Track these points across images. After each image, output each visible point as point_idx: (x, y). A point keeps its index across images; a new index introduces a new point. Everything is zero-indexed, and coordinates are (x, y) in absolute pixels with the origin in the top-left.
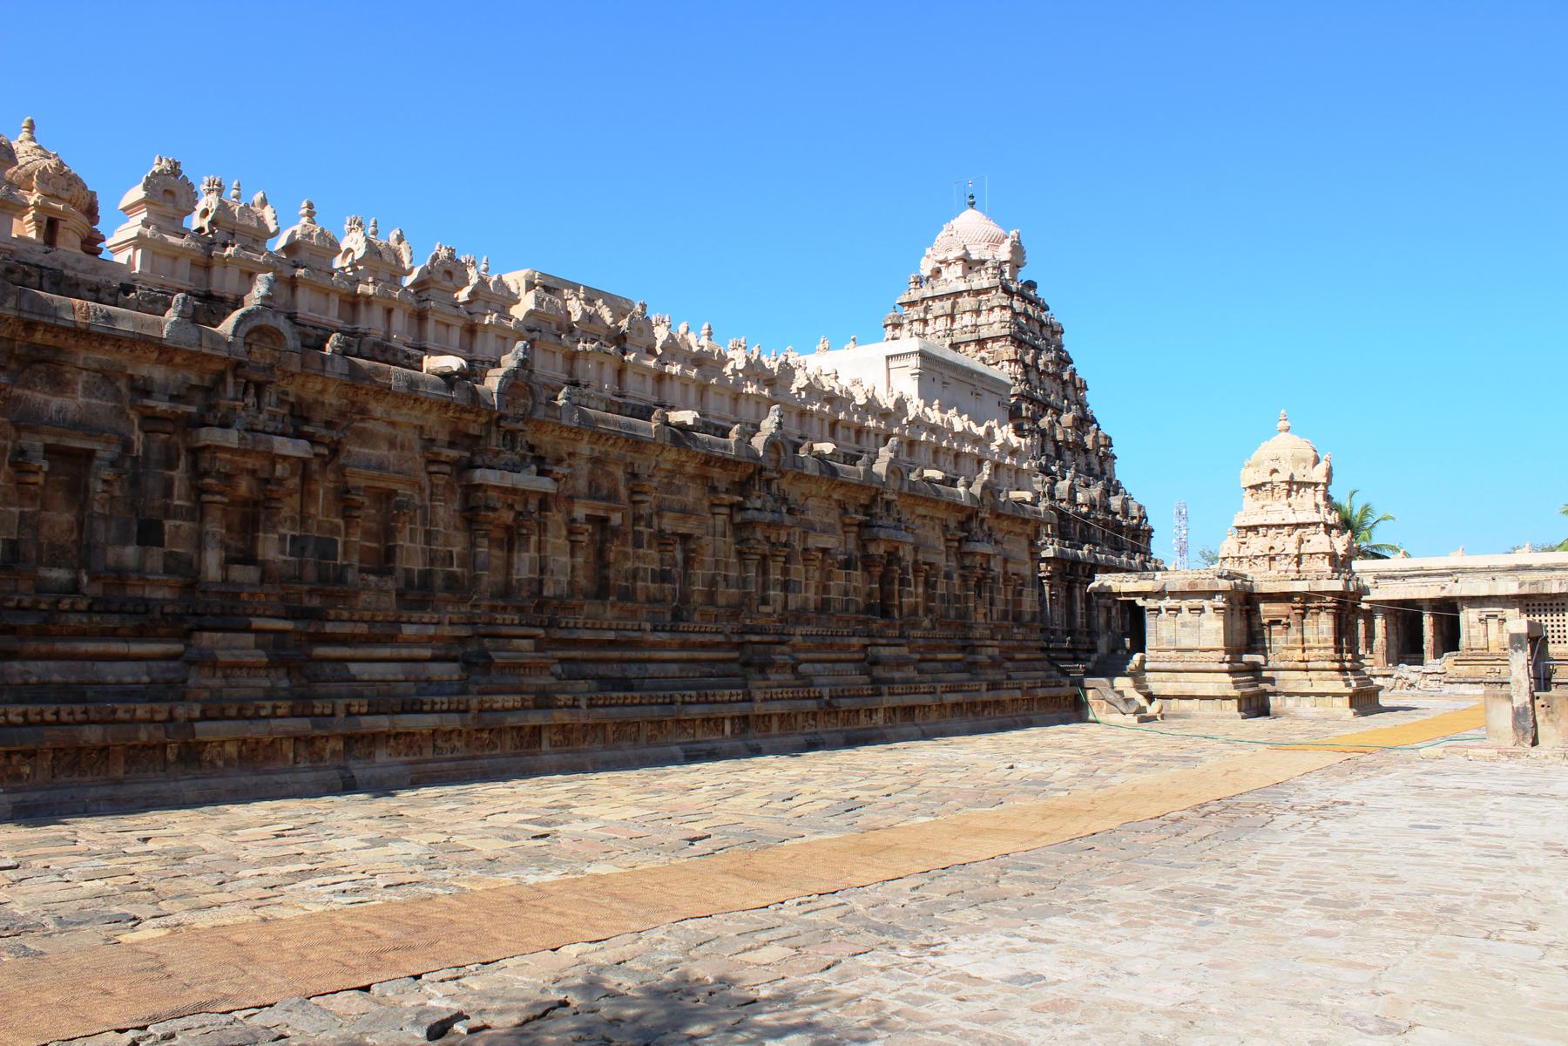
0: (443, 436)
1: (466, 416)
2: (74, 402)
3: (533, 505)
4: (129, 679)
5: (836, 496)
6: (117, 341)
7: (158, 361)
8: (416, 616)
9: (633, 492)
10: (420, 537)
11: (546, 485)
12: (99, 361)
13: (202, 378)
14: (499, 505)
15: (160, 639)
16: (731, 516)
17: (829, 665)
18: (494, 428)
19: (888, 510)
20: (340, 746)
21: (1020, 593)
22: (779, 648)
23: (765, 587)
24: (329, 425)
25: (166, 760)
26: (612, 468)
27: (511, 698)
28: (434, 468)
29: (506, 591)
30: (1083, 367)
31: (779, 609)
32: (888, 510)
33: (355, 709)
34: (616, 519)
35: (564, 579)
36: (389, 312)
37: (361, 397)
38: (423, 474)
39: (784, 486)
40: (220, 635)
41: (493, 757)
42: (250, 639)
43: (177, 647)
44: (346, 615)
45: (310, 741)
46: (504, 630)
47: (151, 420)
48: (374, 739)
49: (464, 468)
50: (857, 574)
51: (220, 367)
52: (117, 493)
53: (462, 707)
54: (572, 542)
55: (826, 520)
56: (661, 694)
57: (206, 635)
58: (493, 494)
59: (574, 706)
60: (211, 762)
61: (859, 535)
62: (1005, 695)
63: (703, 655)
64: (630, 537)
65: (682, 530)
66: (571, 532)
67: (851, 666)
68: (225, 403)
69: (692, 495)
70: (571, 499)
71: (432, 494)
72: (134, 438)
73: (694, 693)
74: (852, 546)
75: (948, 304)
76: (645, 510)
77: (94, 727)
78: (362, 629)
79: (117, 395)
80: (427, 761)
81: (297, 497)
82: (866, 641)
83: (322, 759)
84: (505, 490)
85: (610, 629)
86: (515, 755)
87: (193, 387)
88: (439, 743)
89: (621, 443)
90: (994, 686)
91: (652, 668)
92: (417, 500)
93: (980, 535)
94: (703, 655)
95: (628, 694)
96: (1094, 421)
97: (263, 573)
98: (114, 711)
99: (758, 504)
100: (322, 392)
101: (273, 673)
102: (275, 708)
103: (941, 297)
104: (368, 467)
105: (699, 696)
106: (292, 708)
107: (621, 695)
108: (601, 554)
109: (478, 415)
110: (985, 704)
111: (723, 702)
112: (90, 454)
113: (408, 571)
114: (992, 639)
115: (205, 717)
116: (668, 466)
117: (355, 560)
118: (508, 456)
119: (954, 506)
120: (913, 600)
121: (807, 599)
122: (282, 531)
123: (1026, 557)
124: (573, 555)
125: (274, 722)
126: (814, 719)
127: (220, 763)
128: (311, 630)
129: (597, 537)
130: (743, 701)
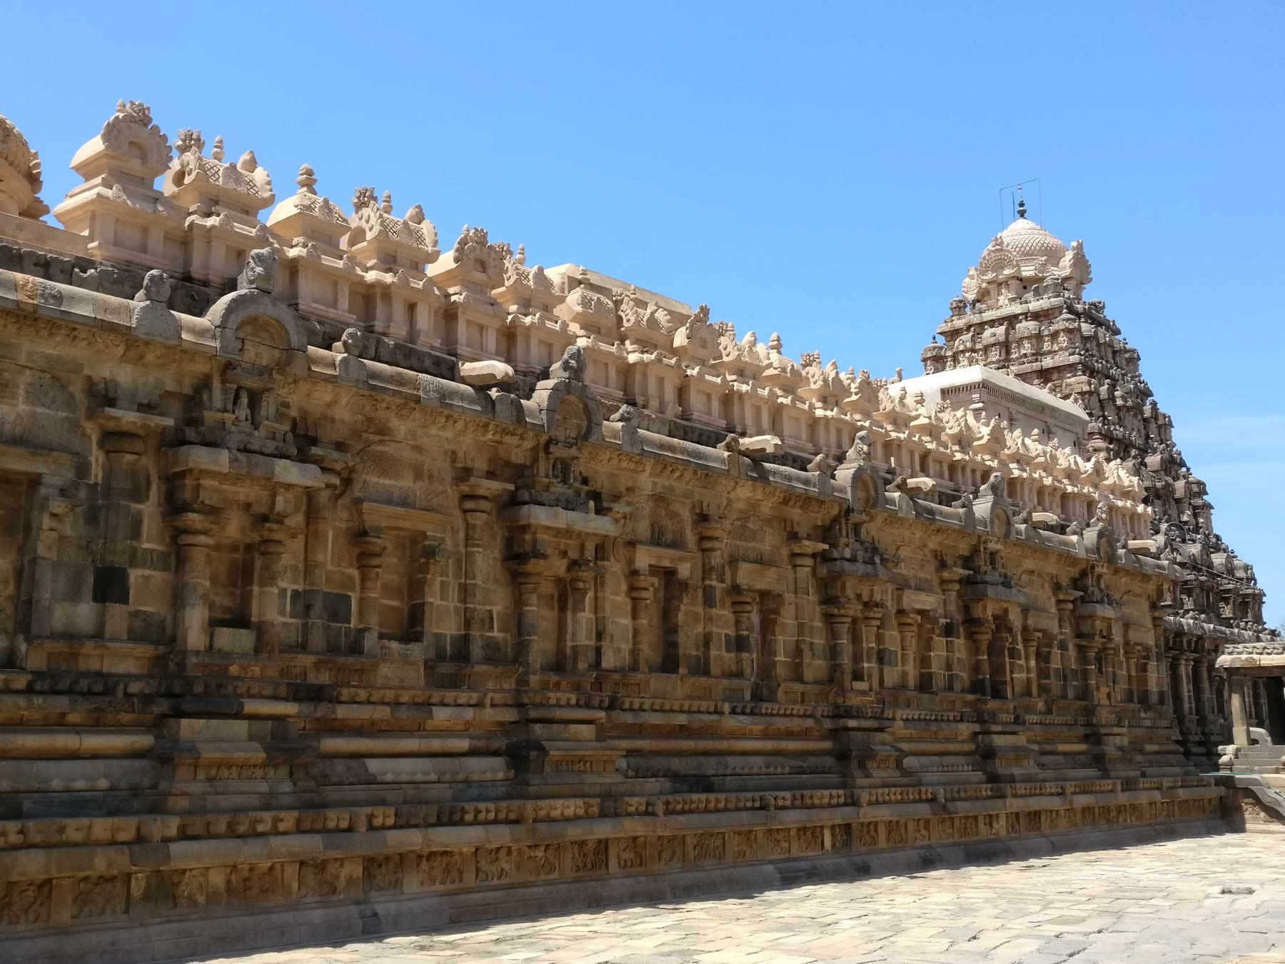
0: (481, 465)
1: (508, 439)
2: (13, 411)
3: (590, 553)
4: (80, 784)
5: (932, 546)
6: (68, 326)
7: (124, 359)
8: (450, 696)
9: (702, 539)
10: (454, 593)
11: (602, 526)
12: (46, 356)
13: (179, 383)
14: (549, 551)
15: (120, 728)
16: (814, 569)
17: (936, 759)
18: (542, 455)
19: (993, 563)
20: (358, 871)
21: (1144, 668)
22: (879, 736)
24: (340, 446)
25: (128, 897)
26: (677, 507)
27: (572, 802)
28: (469, 505)
29: (559, 664)
30: (1165, 400)
31: (876, 685)
32: (993, 563)
33: (378, 822)
34: (684, 570)
35: (626, 647)
36: (412, 308)
37: (381, 414)
38: (457, 513)
39: (873, 533)
40: (202, 722)
41: (551, 883)
42: (241, 727)
43: (145, 741)
44: (363, 694)
45: (321, 866)
46: (559, 714)
47: (113, 438)
48: (402, 861)
49: (512, 502)
50: (960, 642)
51: (202, 367)
52: (68, 532)
53: (512, 816)
54: (633, 599)
55: (921, 575)
56: (749, 795)
57: (184, 722)
59: (647, 813)
60: (190, 898)
61: (960, 595)
62: (1143, 798)
63: (792, 745)
64: (700, 592)
65: (760, 586)
66: (632, 588)
67: (961, 759)
68: (210, 416)
69: (769, 542)
70: (631, 544)
71: (467, 538)
72: (93, 459)
73: (788, 795)
74: (952, 608)
75: (1001, 330)
76: (717, 559)
77: (33, 852)
78: (383, 713)
79: (70, 403)
80: (468, 891)
81: (301, 537)
82: (977, 728)
83: (334, 890)
84: (557, 532)
85: (682, 711)
86: (577, 880)
87: (170, 394)
88: (483, 864)
89: (688, 474)
90: (1128, 785)
91: (733, 761)
92: (449, 544)
93: (1098, 595)
94: (792, 745)
95: (712, 796)
96: (1182, 464)
97: (260, 638)
98: (62, 830)
99: (847, 553)
101: (271, 772)
102: (276, 821)
103: (992, 323)
104: (389, 502)
105: (794, 798)
106: (299, 821)
107: (703, 796)
108: (667, 615)
109: (522, 438)
110: (1120, 810)
111: (822, 807)
112: (34, 481)
114: (1119, 725)
115: (184, 836)
116: (741, 505)
117: (373, 620)
118: (559, 489)
119: (1067, 558)
120: (1024, 676)
121: (904, 675)
122: (283, 584)
123: (1148, 622)
124: (635, 615)
125: (275, 841)
126: (927, 828)
127: (201, 899)
128: (319, 714)
129: (661, 594)
130: (845, 804)
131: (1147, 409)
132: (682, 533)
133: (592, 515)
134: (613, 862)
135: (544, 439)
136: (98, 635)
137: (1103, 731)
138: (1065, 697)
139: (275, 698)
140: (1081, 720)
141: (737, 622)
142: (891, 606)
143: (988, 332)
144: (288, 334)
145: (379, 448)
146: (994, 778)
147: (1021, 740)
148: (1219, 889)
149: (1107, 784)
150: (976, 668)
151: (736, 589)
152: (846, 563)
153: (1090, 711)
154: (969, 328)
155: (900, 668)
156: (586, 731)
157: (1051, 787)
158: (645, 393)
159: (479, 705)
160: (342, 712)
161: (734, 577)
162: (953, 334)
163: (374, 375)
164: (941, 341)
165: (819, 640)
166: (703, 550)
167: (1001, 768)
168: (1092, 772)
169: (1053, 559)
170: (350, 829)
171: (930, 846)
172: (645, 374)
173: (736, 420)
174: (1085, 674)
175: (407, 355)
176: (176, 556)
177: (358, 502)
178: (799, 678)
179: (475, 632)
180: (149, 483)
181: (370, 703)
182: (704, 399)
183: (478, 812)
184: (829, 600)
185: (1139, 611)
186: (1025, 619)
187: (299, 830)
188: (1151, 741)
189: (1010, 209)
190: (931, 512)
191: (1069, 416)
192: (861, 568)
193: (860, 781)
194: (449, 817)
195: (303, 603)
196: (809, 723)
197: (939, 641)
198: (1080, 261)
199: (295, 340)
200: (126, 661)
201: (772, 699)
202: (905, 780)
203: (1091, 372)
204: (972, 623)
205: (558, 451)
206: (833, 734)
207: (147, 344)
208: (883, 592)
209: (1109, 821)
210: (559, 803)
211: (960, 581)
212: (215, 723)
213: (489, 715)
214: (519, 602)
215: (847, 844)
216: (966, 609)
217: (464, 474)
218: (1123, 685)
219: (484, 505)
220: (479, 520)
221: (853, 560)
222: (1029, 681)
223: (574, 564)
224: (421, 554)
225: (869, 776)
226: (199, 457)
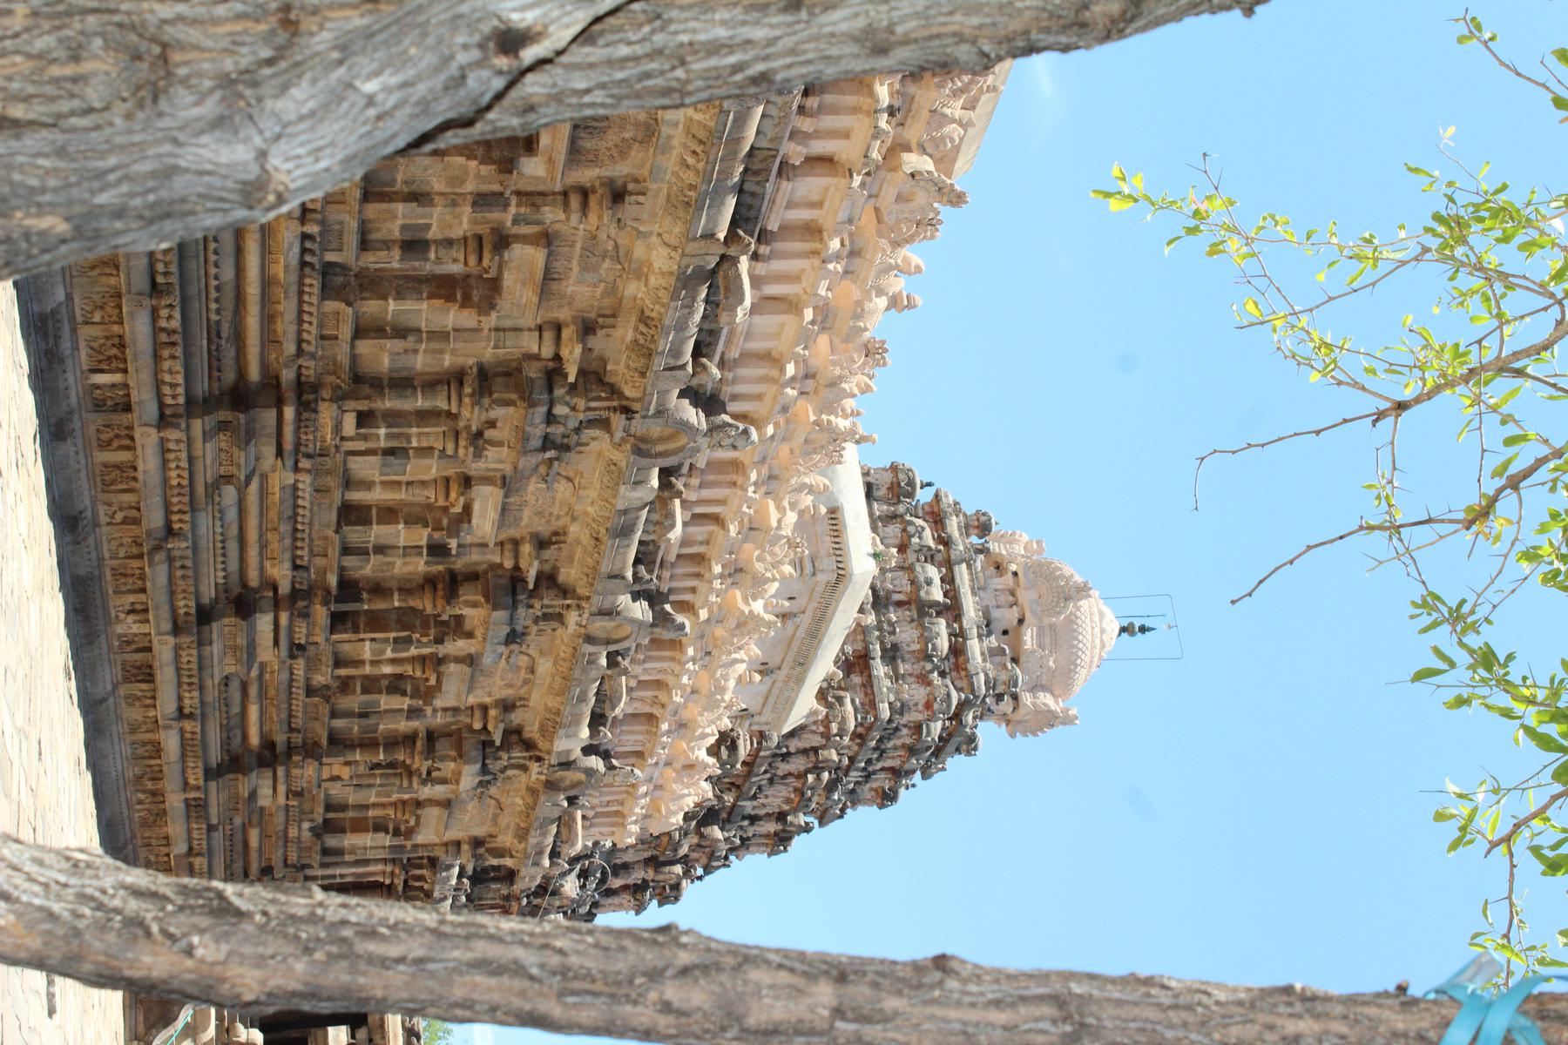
5: (574, 529)
9: (585, 193)
16: (537, 357)
17: (234, 531)
19: (546, 617)
21: (379, 827)
22: (269, 451)
26: (636, 153)
31: (349, 446)
34: (533, 169)
39: (594, 445)
50: (420, 565)
55: (526, 513)
56: (174, 268)
64: (496, 188)
65: (508, 278)
67: (233, 566)
69: (581, 291)
73: (176, 324)
74: (475, 556)
75: (937, 594)
76: (551, 215)
82: (284, 588)
89: (689, 177)
90: (196, 808)
93: (495, 766)
96: (708, 870)
99: (560, 410)
103: (949, 580)
111: (157, 372)
116: (639, 252)
119: (552, 726)
121: (368, 485)
123: (452, 834)
126: (125, 521)
130: (162, 406)
131: (802, 819)
132: (595, 162)
137: (281, 771)
138: (334, 714)
140: (297, 739)
141: (449, 243)
142: (476, 468)
143: (933, 572)
147: (266, 653)
149: (196, 777)
151: (502, 241)
152: (544, 409)
153: (311, 751)
154: (946, 542)
155: (377, 478)
157: (191, 700)
158: (821, 110)
161: (524, 239)
162: (937, 517)
164: (924, 496)
165: (421, 362)
166: (565, 194)
167: (224, 628)
168: (215, 755)
169: (553, 703)
171: (97, 525)
172: (855, 110)
173: (779, 246)
174: (369, 744)
178: (360, 332)
182: (815, 198)
184: (486, 380)
185: (470, 823)
186: (458, 660)
188: (264, 836)
190: (625, 532)
191: (790, 703)
192: (537, 431)
193: (197, 426)
196: (290, 348)
197: (422, 536)
198: (1050, 720)
201: (327, 292)
202: (200, 490)
203: (860, 737)
204: (452, 584)
206: (271, 383)
208: (496, 459)
209: (139, 778)
211: (517, 568)
215: (99, 406)
216: (473, 576)
218: (353, 798)
221: (550, 418)
225: (206, 436)
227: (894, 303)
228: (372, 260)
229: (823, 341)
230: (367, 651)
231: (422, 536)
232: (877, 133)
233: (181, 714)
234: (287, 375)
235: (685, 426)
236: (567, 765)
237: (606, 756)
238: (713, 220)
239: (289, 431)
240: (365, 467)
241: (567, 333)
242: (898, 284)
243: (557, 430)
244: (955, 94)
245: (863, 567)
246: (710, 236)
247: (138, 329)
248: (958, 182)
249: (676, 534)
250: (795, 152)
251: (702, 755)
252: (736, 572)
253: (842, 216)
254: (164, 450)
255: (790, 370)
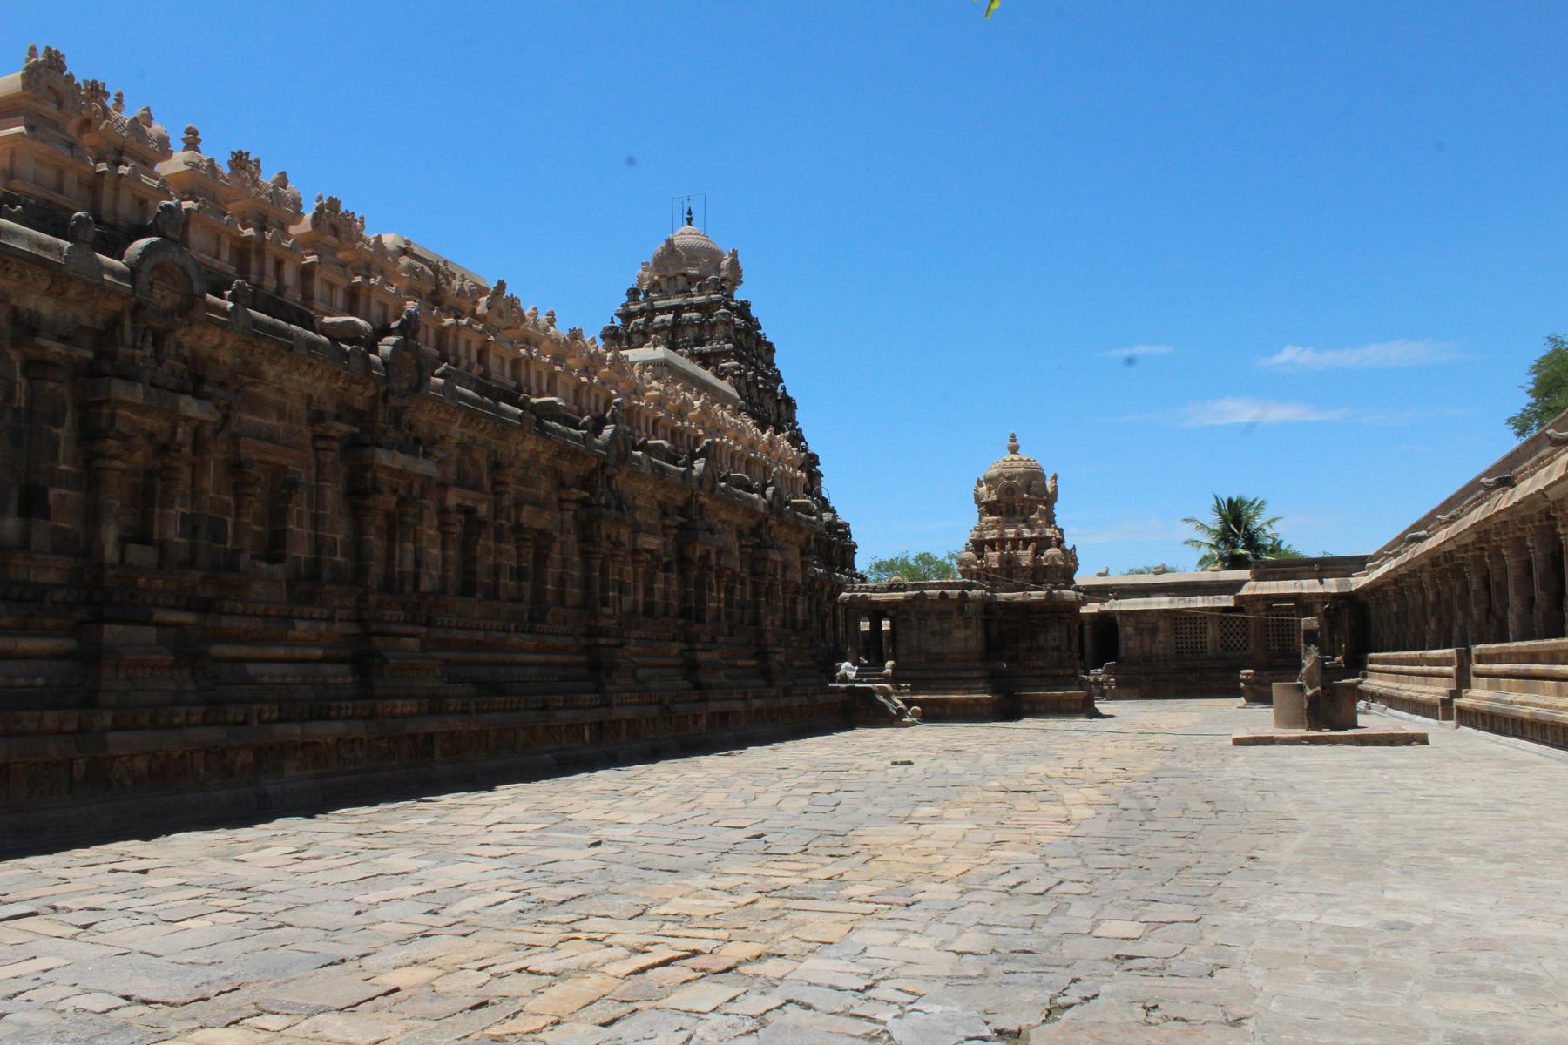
0: (330, 408)
4: (21, 681)
9: (496, 483)
10: (307, 522)
15: (45, 633)
19: (701, 513)
20: (250, 758)
21: (794, 601)
23: (604, 589)
24: (222, 385)
28: (321, 444)
33: (266, 715)
34: (483, 510)
36: (279, 264)
38: (311, 450)
40: (121, 627)
42: (150, 633)
43: (68, 644)
44: (240, 607)
47: (36, 367)
51: (115, 305)
57: (106, 627)
58: (382, 475)
63: (557, 658)
65: (537, 525)
66: (442, 524)
68: (123, 351)
69: (543, 488)
70: (444, 485)
71: (318, 474)
74: (670, 548)
75: (670, 317)
82: (684, 646)
84: (392, 471)
85: (478, 629)
87: (83, 328)
89: (490, 427)
90: (787, 692)
92: (303, 479)
94: (557, 658)
96: (803, 439)
99: (603, 501)
100: (221, 345)
102: (188, 715)
103: (662, 311)
104: (258, 438)
108: (467, 547)
113: (297, 559)
115: (116, 727)
116: (525, 456)
117: (247, 543)
118: (392, 434)
120: (714, 605)
121: (635, 602)
124: (444, 547)
127: (128, 782)
131: (779, 390)
133: (421, 459)
134: (437, 751)
135: (382, 389)
136: (25, 545)
139: (175, 608)
141: (519, 555)
142: (628, 547)
143: (658, 319)
144: (190, 279)
145: (251, 389)
146: (697, 686)
147: (714, 655)
148: (888, 763)
150: (685, 598)
151: (518, 528)
154: (642, 311)
156: (412, 643)
158: (456, 354)
159: (330, 619)
160: (226, 622)
161: (518, 518)
163: (257, 323)
164: (618, 322)
165: (577, 573)
166: (496, 494)
170: (244, 723)
172: (456, 337)
174: (757, 606)
175: (275, 306)
176: (91, 476)
177: (235, 437)
179: (325, 557)
180: (65, 409)
181: (244, 614)
183: (340, 708)
185: (794, 556)
186: (719, 559)
187: (205, 723)
189: (680, 216)
190: (662, 468)
191: (725, 394)
192: (614, 513)
193: (610, 688)
194: (320, 714)
195: (191, 525)
196: (570, 640)
197: (661, 575)
198: (734, 264)
199: (197, 286)
200: (49, 572)
203: (740, 359)
204: (683, 561)
205: (394, 401)
207: (70, 279)
208: (625, 536)
210: (399, 702)
212: (129, 628)
213: (338, 627)
214: (358, 530)
216: (680, 550)
217: (317, 417)
219: (336, 445)
220: (329, 457)
221: (607, 506)
222: (718, 609)
223: (402, 501)
224: (284, 487)
226: (120, 389)
227: (552, 322)
228: (527, 597)
229: (570, 362)
230: (714, 605)
231: (661, 575)
232: (469, 325)
233: (744, 699)
234: (583, 641)
235: (613, 435)
236: (770, 505)
237: (765, 486)
238: (514, 415)
239: (611, 641)
240: (627, 601)
241: (564, 496)
242: (542, 318)
243: (613, 503)
244: (449, 283)
245: (660, 352)
246: (520, 417)
247: (565, 716)
248: (492, 284)
249: (666, 444)
250: (477, 370)
251: (766, 436)
252: (681, 413)
253: (509, 347)
254: (621, 705)
255: (584, 379)
